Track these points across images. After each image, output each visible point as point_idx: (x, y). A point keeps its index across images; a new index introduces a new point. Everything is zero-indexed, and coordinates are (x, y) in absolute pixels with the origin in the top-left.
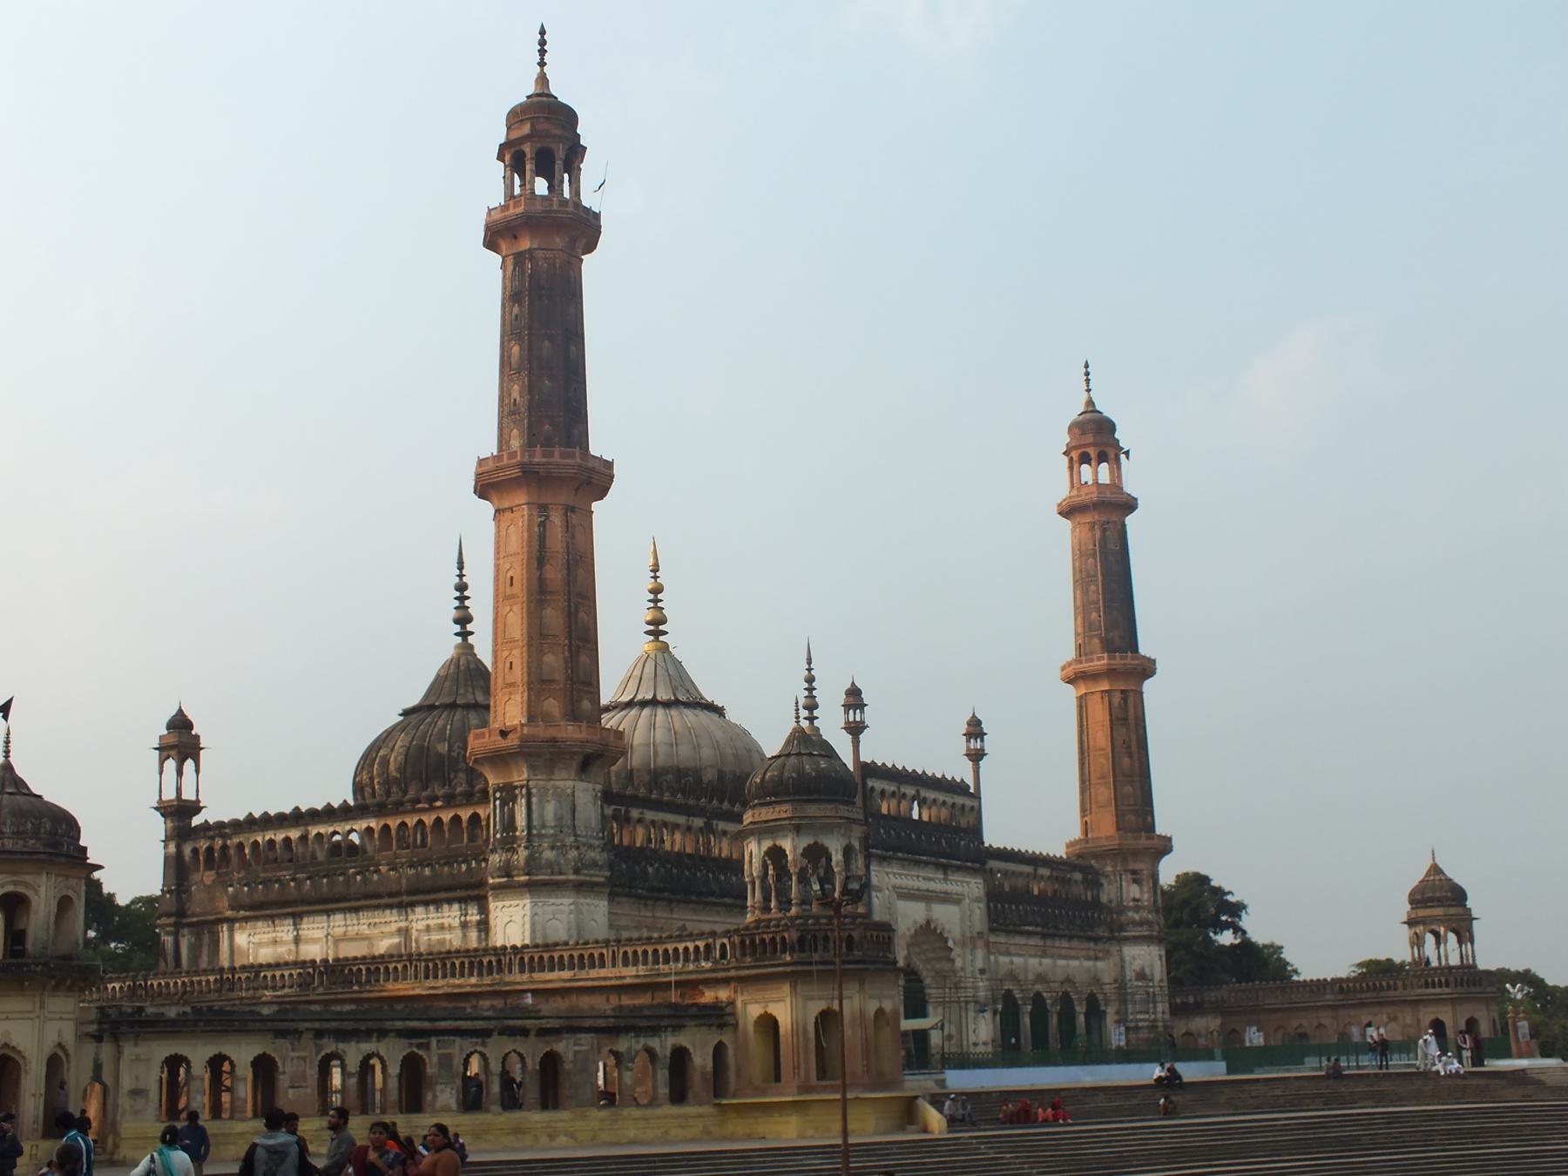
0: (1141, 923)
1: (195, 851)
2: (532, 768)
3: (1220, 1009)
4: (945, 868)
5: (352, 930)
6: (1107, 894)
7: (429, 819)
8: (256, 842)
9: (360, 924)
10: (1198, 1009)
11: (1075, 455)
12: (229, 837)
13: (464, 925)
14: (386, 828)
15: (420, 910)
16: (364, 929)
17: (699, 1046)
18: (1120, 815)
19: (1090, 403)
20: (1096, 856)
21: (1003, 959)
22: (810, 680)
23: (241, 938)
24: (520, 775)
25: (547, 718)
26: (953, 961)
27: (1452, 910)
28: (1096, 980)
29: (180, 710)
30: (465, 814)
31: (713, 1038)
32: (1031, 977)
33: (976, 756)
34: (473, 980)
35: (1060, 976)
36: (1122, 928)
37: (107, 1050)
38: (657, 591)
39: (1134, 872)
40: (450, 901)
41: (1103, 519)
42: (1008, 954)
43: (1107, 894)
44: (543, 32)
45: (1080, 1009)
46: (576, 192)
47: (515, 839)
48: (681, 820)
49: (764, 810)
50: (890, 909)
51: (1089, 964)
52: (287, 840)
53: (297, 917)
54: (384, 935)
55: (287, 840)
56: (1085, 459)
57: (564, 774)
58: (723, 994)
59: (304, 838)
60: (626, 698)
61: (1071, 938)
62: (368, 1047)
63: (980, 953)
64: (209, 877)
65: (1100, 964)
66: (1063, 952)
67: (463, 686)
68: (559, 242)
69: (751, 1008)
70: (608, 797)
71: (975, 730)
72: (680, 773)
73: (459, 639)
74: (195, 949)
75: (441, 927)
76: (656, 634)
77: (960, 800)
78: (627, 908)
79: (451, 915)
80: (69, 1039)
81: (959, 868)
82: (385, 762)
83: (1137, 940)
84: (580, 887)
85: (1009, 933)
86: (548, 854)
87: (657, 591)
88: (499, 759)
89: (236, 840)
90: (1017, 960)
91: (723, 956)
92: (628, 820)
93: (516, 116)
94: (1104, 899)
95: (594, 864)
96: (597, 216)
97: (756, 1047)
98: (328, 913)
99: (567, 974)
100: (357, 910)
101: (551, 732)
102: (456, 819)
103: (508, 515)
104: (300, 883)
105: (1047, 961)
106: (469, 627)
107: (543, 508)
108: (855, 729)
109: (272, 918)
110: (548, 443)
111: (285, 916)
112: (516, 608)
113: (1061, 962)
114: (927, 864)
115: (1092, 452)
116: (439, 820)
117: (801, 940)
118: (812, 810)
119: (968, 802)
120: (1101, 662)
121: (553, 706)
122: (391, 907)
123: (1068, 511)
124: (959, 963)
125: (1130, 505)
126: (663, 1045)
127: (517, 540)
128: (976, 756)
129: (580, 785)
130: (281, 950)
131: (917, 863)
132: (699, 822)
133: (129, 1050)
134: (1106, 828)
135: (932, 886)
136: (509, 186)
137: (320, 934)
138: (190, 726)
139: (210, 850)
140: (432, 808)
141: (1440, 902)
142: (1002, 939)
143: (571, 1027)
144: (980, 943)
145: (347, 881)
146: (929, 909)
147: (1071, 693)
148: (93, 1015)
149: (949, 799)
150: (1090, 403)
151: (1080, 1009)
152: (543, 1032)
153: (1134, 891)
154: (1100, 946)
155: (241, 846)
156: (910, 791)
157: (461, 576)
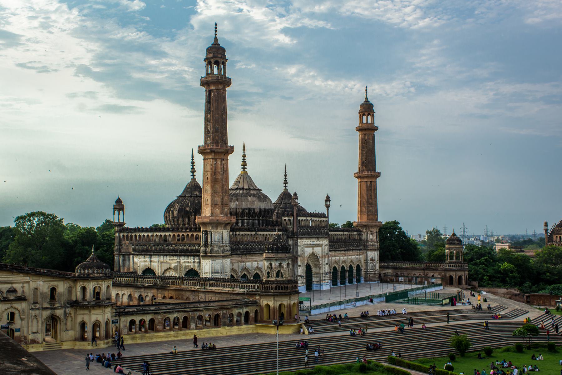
0: (372, 245)
1: (123, 236)
2: (213, 227)
3: (394, 268)
4: (318, 238)
5: (165, 261)
6: (364, 237)
7: (185, 234)
8: (140, 235)
9: (167, 259)
10: (388, 268)
11: (361, 114)
12: (132, 233)
13: (194, 262)
14: (174, 235)
15: (182, 258)
16: (168, 260)
17: (251, 310)
18: (368, 215)
19: (367, 98)
20: (362, 227)
21: (334, 258)
22: (286, 176)
23: (136, 260)
24: (209, 229)
25: (216, 215)
27: (457, 246)
28: (360, 261)
29: (119, 198)
30: (195, 234)
31: (254, 309)
32: (341, 262)
33: (328, 206)
34: (198, 287)
35: (349, 261)
36: (367, 246)
37: (117, 318)
38: (244, 156)
39: (371, 231)
40: (191, 256)
41: (368, 133)
42: (335, 256)
43: (364, 237)
44: (216, 25)
45: (355, 268)
46: (225, 72)
47: (208, 244)
48: (249, 233)
49: (268, 254)
50: (303, 251)
52: (148, 235)
53: (151, 256)
54: (173, 263)
55: (148, 235)
56: (364, 115)
57: (220, 228)
58: (257, 297)
59: (152, 235)
60: (236, 187)
61: (353, 250)
62: (175, 315)
63: (326, 259)
64: (127, 242)
67: (193, 189)
68: (220, 87)
69: (264, 302)
70: (231, 231)
71: (328, 199)
72: (249, 209)
73: (192, 177)
74: (124, 260)
75: (188, 262)
76: (244, 168)
77: (323, 219)
78: (235, 258)
79: (191, 259)
80: (110, 317)
81: (322, 237)
82: (173, 212)
83: (371, 250)
84: (223, 257)
85: (335, 251)
86: (216, 249)
87: (244, 156)
88: (204, 224)
89: (134, 234)
90: (337, 258)
91: (258, 288)
92: (236, 235)
93: (209, 50)
94: (363, 238)
95: (227, 251)
96: (230, 79)
97: (265, 310)
98: (159, 255)
99: (221, 288)
100: (166, 255)
101: (217, 218)
102: (192, 235)
103: (207, 161)
104: (152, 247)
105: (346, 257)
106: (195, 173)
107: (216, 160)
109: (144, 255)
110: (217, 143)
111: (148, 255)
112: (209, 185)
115: (366, 114)
116: (188, 235)
117: (276, 287)
118: (280, 255)
119: (325, 219)
120: (365, 173)
121: (218, 211)
122: (175, 255)
123: (359, 130)
124: (321, 262)
125: (376, 129)
126: (243, 311)
127: (209, 168)
128: (328, 206)
129: (224, 231)
130: (146, 263)
131: (310, 238)
132: (254, 233)
133: (123, 319)
134: (365, 219)
135: (315, 243)
136: (207, 70)
137: (157, 261)
138: (121, 202)
139: (127, 236)
140: (186, 232)
141: (454, 244)
143: (222, 308)
144: (327, 256)
145: (164, 248)
146: (313, 249)
147: (357, 181)
148: (114, 311)
149: (320, 219)
150: (367, 98)
151: (355, 268)
152: (216, 309)
153: (371, 237)
155: (136, 236)
156: (309, 218)
157: (193, 160)
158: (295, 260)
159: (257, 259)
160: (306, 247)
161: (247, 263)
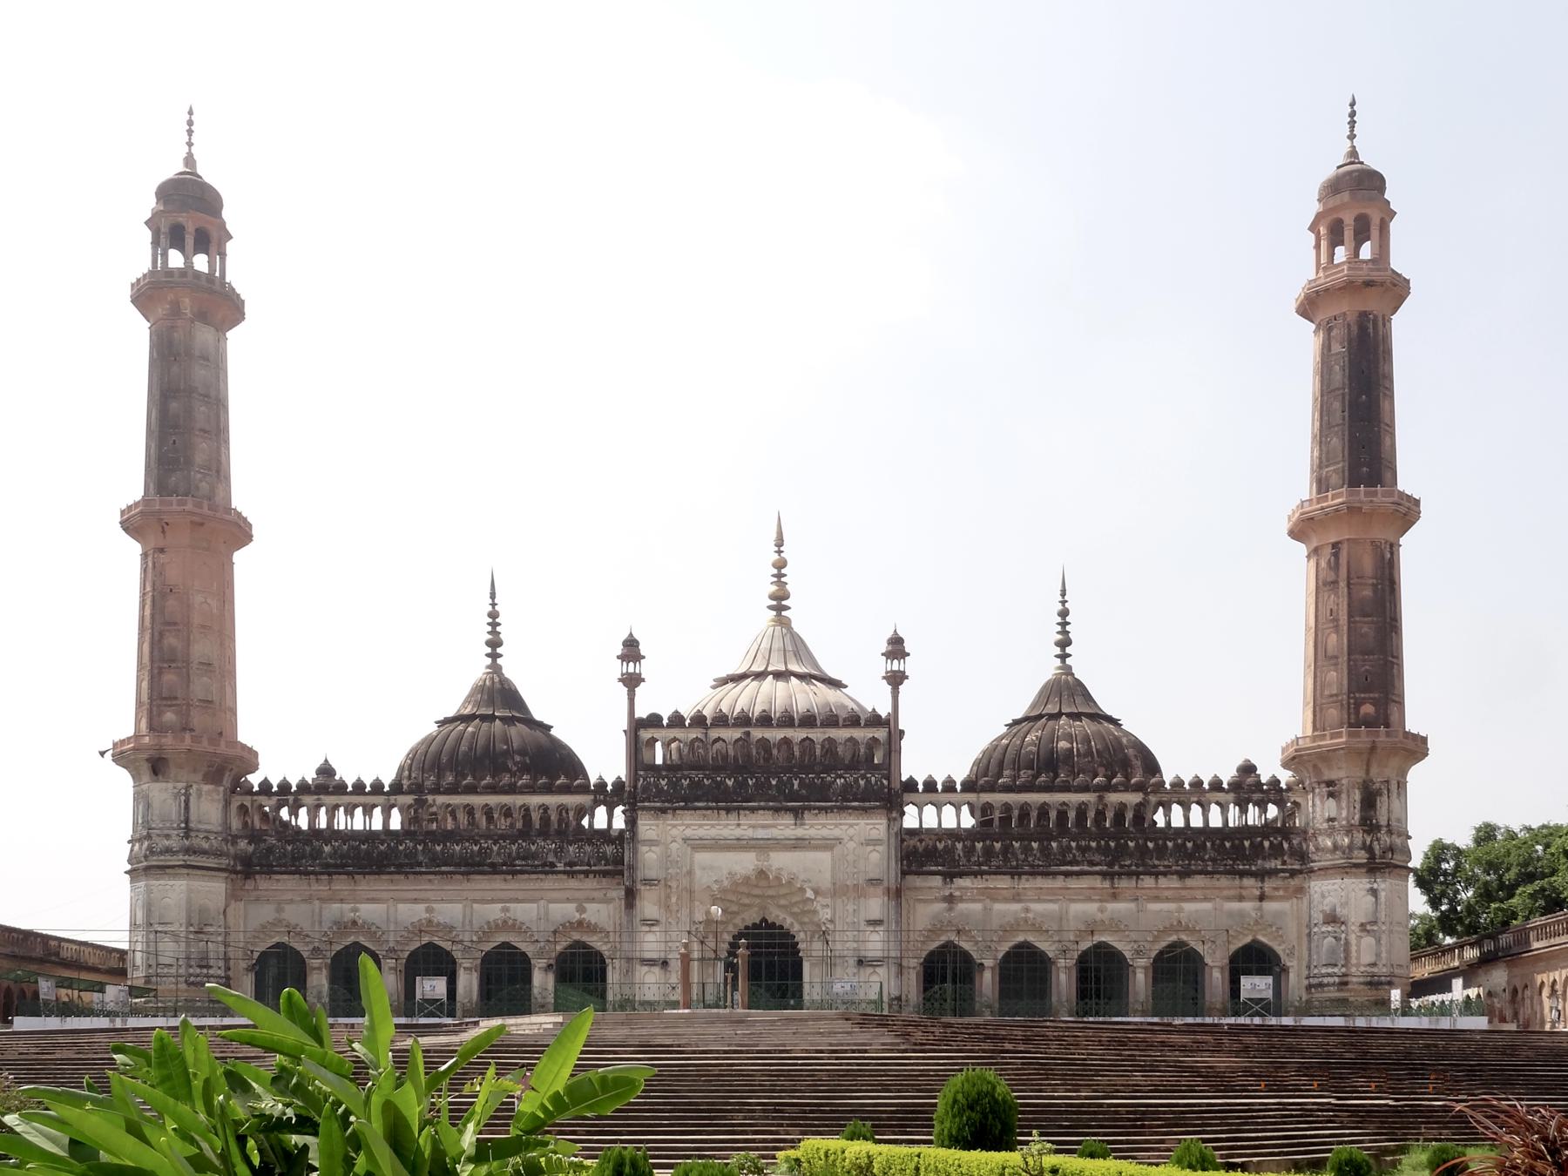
4: (797, 813)
26: (815, 912)
33: (896, 680)
42: (1016, 898)
51: (1248, 906)
61: (1184, 875)
65: (1270, 906)
66: (1167, 893)
71: (896, 648)
81: (826, 810)
85: (1012, 875)
105: (1112, 907)
108: (632, 682)
113: (1154, 907)
114: (753, 810)
124: (825, 914)
128: (896, 680)
131: (728, 810)
135: (775, 833)
142: (1003, 882)
154: (1269, 884)
158: (631, 896)
159: (430, 895)
160: (695, 848)
161: (363, 907)
